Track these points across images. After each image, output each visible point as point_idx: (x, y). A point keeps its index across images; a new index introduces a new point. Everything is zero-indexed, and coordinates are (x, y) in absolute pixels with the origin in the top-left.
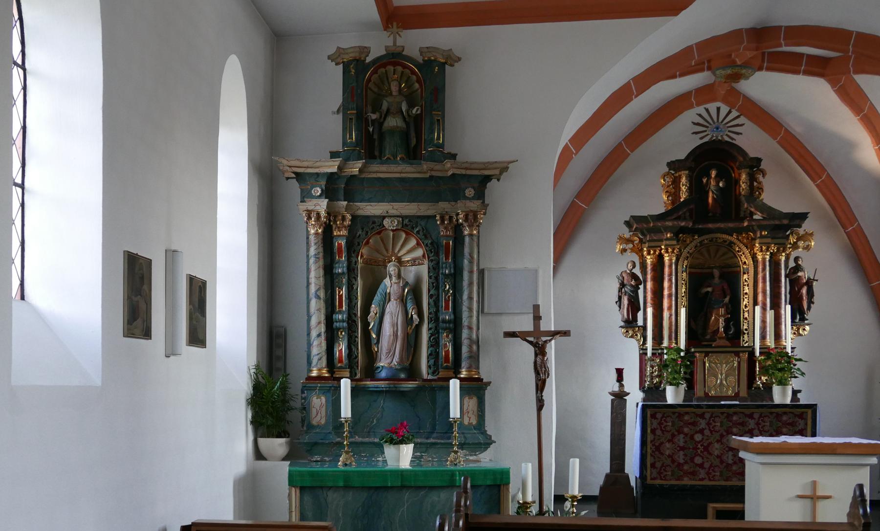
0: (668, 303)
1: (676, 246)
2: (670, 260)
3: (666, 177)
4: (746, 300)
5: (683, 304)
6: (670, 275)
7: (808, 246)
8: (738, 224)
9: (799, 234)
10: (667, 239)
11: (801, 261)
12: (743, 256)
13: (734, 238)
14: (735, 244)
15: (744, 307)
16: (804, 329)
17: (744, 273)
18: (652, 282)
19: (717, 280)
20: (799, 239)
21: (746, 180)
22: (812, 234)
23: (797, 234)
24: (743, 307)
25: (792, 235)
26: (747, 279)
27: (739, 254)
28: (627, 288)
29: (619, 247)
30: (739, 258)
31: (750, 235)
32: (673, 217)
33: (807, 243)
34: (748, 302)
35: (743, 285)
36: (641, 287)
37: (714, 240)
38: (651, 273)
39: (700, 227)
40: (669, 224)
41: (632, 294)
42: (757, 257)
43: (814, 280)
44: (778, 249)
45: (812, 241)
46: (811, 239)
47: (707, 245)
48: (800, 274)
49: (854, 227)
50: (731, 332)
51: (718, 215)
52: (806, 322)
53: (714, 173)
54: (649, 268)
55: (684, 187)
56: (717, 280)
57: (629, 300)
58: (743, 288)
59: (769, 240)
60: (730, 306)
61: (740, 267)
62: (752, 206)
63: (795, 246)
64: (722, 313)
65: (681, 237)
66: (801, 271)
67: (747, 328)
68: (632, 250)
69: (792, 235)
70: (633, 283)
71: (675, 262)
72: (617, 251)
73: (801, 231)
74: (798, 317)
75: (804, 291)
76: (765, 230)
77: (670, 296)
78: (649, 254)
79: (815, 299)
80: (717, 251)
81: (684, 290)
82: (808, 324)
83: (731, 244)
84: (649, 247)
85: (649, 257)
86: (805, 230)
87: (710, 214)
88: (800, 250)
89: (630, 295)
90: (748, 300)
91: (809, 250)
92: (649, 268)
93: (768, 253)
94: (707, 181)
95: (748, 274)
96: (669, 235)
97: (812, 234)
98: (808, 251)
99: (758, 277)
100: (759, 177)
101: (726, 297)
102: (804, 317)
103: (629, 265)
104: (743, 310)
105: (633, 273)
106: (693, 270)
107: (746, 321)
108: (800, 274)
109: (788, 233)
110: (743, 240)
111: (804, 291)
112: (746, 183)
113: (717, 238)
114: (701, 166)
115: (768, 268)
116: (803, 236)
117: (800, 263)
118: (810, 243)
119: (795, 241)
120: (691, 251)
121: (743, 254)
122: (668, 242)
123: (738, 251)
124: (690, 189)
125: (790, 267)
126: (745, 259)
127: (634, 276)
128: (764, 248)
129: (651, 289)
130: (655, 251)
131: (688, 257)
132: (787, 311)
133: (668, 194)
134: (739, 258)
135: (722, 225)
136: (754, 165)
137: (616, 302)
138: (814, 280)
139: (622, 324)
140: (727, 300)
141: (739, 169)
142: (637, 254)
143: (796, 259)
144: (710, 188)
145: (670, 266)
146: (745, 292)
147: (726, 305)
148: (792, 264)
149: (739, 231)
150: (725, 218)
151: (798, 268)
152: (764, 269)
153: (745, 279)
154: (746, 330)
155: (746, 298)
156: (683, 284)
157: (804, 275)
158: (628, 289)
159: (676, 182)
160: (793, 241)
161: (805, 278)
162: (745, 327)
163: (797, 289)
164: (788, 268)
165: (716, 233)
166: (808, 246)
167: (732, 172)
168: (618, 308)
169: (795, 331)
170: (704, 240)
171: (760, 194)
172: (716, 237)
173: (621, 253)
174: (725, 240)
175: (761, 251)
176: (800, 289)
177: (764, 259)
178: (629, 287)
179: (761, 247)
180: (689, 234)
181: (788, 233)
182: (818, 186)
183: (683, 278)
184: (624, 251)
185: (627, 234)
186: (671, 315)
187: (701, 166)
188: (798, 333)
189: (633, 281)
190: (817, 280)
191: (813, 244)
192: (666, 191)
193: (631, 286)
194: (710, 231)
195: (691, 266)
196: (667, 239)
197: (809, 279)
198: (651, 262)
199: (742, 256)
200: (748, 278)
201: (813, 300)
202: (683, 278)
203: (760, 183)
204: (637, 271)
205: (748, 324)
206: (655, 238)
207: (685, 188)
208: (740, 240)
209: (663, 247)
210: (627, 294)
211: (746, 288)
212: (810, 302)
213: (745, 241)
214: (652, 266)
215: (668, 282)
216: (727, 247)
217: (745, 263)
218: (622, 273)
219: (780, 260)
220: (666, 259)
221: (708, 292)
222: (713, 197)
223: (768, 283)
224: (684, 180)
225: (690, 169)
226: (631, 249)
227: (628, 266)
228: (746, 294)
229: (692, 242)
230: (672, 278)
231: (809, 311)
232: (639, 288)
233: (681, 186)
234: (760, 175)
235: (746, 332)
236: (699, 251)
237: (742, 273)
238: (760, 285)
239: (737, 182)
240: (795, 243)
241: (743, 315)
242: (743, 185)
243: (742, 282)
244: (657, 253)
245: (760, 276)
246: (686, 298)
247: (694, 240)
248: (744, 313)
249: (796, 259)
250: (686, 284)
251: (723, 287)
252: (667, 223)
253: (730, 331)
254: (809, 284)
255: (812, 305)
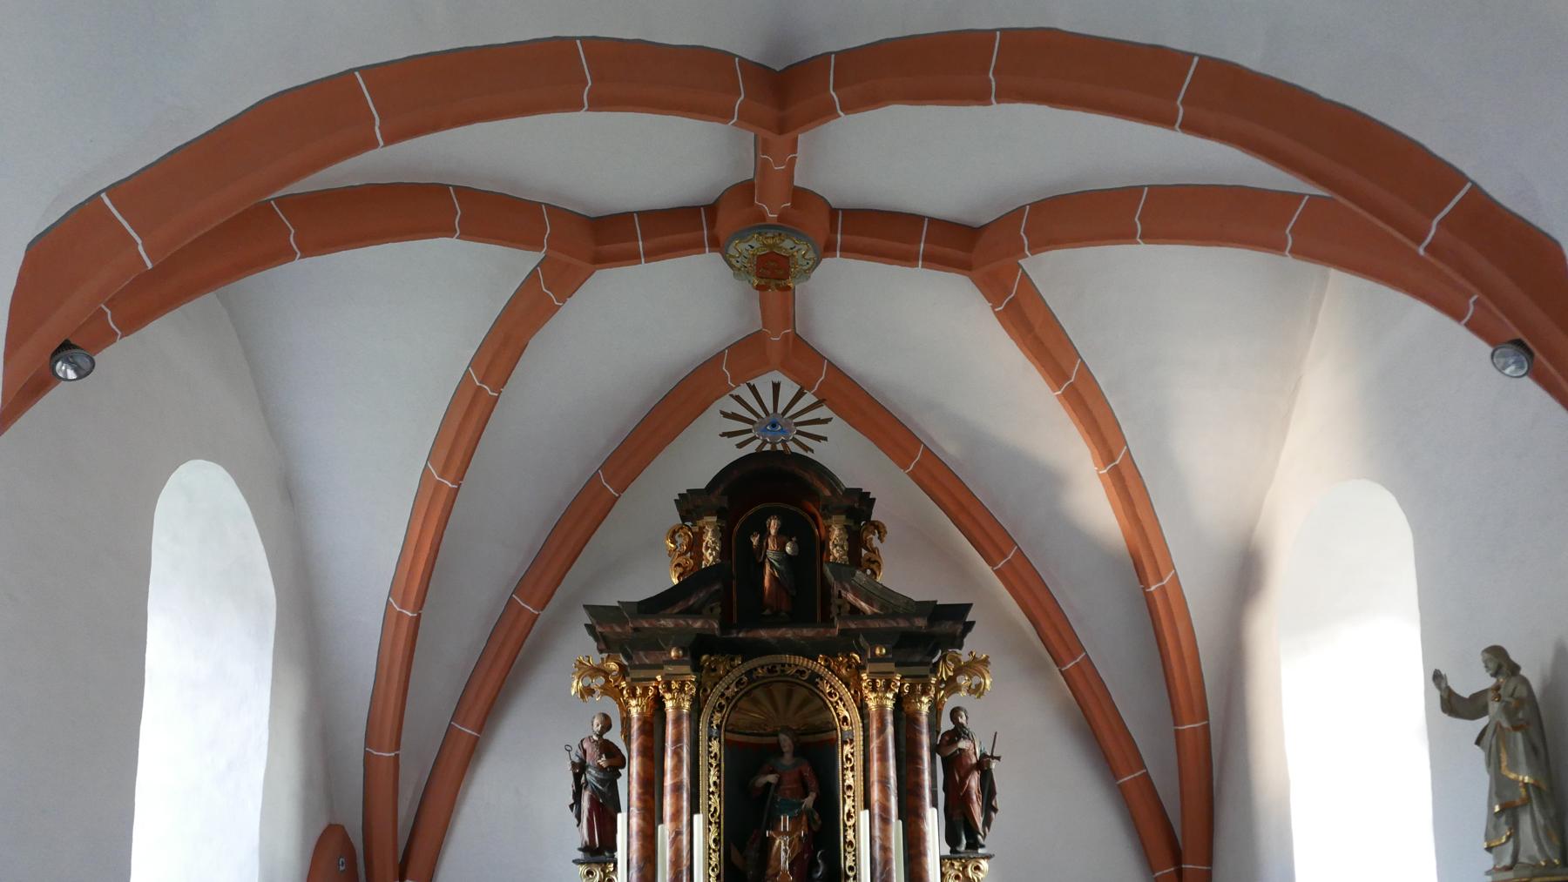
0: (672, 805)
1: (688, 677)
2: (678, 708)
3: (677, 536)
4: (849, 802)
5: (712, 809)
6: (678, 740)
7: (978, 686)
8: (822, 630)
9: (960, 661)
10: (671, 662)
11: (964, 718)
12: (841, 704)
13: (819, 665)
14: (822, 679)
15: (845, 818)
16: (977, 868)
17: (844, 742)
18: (640, 759)
19: (788, 759)
20: (959, 670)
21: (841, 540)
22: (985, 662)
23: (956, 660)
24: (842, 817)
25: (945, 662)
26: (850, 756)
27: (831, 699)
28: (590, 773)
29: (576, 686)
30: (832, 709)
31: (855, 659)
32: (676, 610)
33: (976, 680)
34: (853, 807)
35: (843, 769)
36: (624, 772)
37: (778, 668)
38: (637, 739)
39: (741, 635)
40: (668, 623)
41: (600, 787)
42: (867, 705)
43: (992, 757)
44: (912, 687)
45: (986, 675)
46: (984, 671)
47: (766, 681)
48: (963, 744)
49: (1078, 660)
50: (820, 874)
51: (783, 614)
52: (980, 851)
53: (773, 526)
54: (635, 727)
55: (710, 551)
56: (788, 759)
57: (592, 800)
58: (844, 775)
59: (891, 667)
60: (816, 816)
61: (836, 729)
62: (847, 586)
63: (951, 686)
64: (785, 827)
65: (706, 661)
66: (964, 738)
67: (852, 864)
68: (606, 691)
69: (945, 662)
70: (603, 762)
71: (690, 715)
72: (573, 693)
73: (964, 655)
74: (964, 841)
75: (974, 781)
76: (882, 644)
77: (677, 788)
78: (634, 696)
79: (999, 801)
80: (789, 695)
81: (713, 779)
82: (987, 857)
83: (815, 678)
84: (633, 680)
85: (633, 702)
86: (972, 653)
87: (767, 612)
88: (963, 693)
89: (595, 791)
90: (854, 801)
91: (982, 694)
92: (635, 727)
93: (890, 695)
94: (760, 541)
95: (851, 744)
96: (673, 654)
97: (985, 662)
98: (979, 697)
99: (871, 747)
100: (871, 539)
101: (806, 795)
102: (976, 840)
103: (596, 721)
104: (845, 825)
105: (607, 741)
106: (729, 736)
107: (849, 849)
108: (963, 744)
109: (934, 660)
110: (839, 669)
111: (974, 781)
112: (842, 547)
113: (783, 665)
114: (750, 513)
115: (890, 730)
116: (968, 665)
117: (962, 720)
118: (982, 680)
119: (951, 674)
120: (729, 693)
121: (841, 699)
122: (670, 669)
123: (830, 694)
124: (724, 553)
125: (942, 732)
126: (846, 710)
127: (607, 749)
128: (880, 683)
129: (638, 774)
130: (645, 690)
131: (721, 707)
132: (933, 823)
133: (680, 570)
134: (832, 709)
135: (789, 633)
136: (858, 507)
137: (571, 807)
138: (992, 757)
139: (580, 855)
140: (809, 801)
141: (826, 517)
142: (616, 698)
143: (955, 714)
144: (765, 556)
145: (678, 721)
146: (847, 783)
147: (809, 813)
148: (946, 725)
149: (830, 649)
150: (799, 616)
151: (959, 732)
152: (882, 730)
153: (847, 755)
154: (851, 868)
155: (849, 797)
156: (712, 765)
157: (972, 748)
158: (591, 775)
159: (695, 545)
160: (946, 672)
161: (975, 754)
162: (849, 863)
163: (957, 778)
164: (938, 733)
165: (780, 653)
166: (978, 686)
167: (814, 526)
168: (576, 821)
169: (957, 872)
170: (756, 669)
171: (874, 573)
172: (784, 661)
173: (582, 696)
174: (801, 669)
175: (874, 689)
176: (964, 778)
177: (881, 708)
178: (593, 772)
179: (874, 682)
180: (723, 655)
181: (934, 660)
182: (998, 573)
183: (710, 752)
184: (588, 691)
185: (596, 659)
186: (678, 833)
187: (750, 513)
188: (964, 875)
189: (604, 758)
190: (998, 758)
191: (988, 682)
192: (676, 563)
193: (600, 768)
194: (764, 649)
195: (728, 727)
196: (671, 662)
197: (983, 755)
198: (641, 714)
199: (838, 704)
200: (852, 754)
201: (993, 803)
202: (710, 752)
203: (873, 551)
204: (615, 736)
205: (854, 855)
206: (647, 661)
207: (711, 554)
208: (830, 669)
209: (659, 678)
210: (589, 787)
211: (849, 774)
212: (989, 808)
213: (844, 671)
214: (640, 723)
215: (672, 757)
216: (806, 684)
217: (845, 718)
218: (582, 741)
219: (918, 712)
220: (669, 704)
221: (768, 784)
222: (772, 575)
223: (892, 763)
224: (709, 538)
225: (720, 513)
226: (602, 687)
227: (592, 722)
228: (849, 787)
229: (728, 672)
230: (681, 748)
231: (989, 829)
232: (619, 775)
233: (704, 550)
234: (874, 534)
235: (851, 874)
236: (748, 693)
237: (840, 743)
238: (875, 766)
239: (824, 545)
240: (952, 680)
241: (845, 837)
242: (835, 551)
243: (840, 759)
244: (650, 694)
245: (874, 745)
246: (719, 796)
247: (733, 667)
248: (845, 831)
249: (955, 714)
250: (718, 765)
251: (801, 773)
252: (662, 622)
253: (817, 872)
254: (983, 766)
255: (993, 814)
